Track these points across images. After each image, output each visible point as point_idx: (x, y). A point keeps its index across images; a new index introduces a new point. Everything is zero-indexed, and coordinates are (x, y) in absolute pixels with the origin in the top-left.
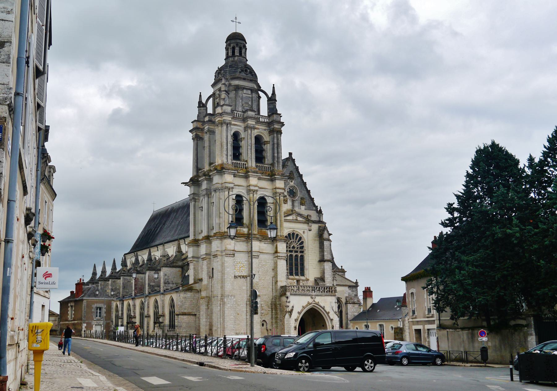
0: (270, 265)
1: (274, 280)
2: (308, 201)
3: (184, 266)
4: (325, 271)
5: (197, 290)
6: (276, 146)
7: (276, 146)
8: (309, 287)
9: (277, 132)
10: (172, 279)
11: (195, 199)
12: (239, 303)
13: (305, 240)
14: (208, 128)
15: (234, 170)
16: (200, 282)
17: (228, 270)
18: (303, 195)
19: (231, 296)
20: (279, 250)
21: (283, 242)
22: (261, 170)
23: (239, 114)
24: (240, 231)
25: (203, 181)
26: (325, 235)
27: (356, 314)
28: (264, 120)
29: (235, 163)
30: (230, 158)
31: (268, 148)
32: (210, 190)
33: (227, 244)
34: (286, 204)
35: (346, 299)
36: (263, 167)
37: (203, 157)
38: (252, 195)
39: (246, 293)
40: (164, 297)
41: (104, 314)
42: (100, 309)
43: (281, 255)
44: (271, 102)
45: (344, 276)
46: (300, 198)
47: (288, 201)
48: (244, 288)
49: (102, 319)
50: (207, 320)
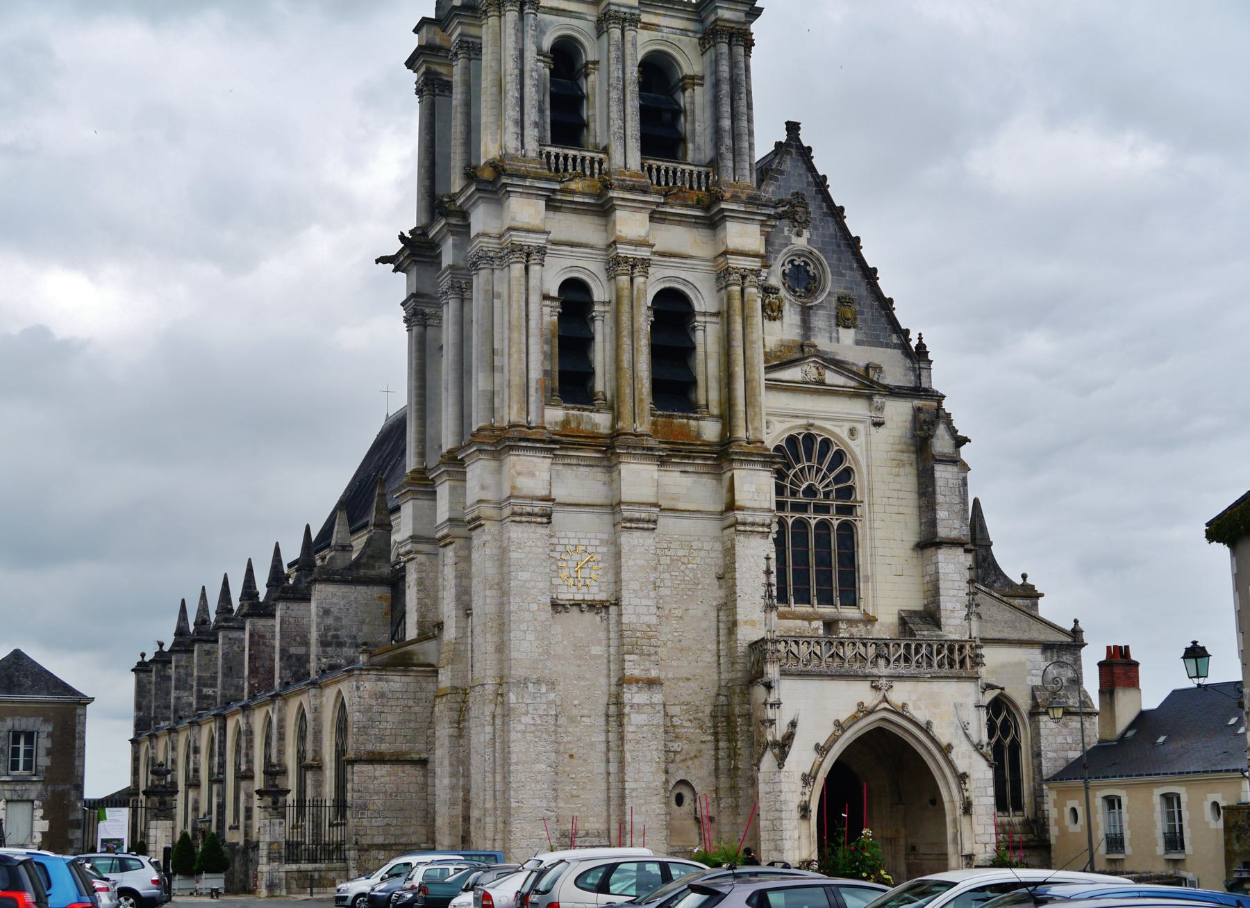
0: (709, 561)
1: (723, 618)
2: (868, 310)
4: (942, 584)
7: (725, 88)
9: (731, 36)
10: (354, 629)
11: (423, 314)
12: (575, 712)
13: (857, 462)
15: (548, 180)
17: (524, 576)
18: (846, 288)
19: (538, 682)
20: (741, 498)
21: (759, 467)
24: (579, 424)
26: (941, 444)
27: (1075, 754)
29: (557, 156)
30: (531, 134)
31: (696, 101)
34: (778, 323)
35: (1034, 698)
39: (605, 672)
40: (321, 696)
41: (43, 761)
42: (30, 737)
43: (750, 519)
45: (1033, 613)
46: (834, 299)
47: (786, 308)
48: (597, 650)
49: (35, 779)
50: (454, 781)
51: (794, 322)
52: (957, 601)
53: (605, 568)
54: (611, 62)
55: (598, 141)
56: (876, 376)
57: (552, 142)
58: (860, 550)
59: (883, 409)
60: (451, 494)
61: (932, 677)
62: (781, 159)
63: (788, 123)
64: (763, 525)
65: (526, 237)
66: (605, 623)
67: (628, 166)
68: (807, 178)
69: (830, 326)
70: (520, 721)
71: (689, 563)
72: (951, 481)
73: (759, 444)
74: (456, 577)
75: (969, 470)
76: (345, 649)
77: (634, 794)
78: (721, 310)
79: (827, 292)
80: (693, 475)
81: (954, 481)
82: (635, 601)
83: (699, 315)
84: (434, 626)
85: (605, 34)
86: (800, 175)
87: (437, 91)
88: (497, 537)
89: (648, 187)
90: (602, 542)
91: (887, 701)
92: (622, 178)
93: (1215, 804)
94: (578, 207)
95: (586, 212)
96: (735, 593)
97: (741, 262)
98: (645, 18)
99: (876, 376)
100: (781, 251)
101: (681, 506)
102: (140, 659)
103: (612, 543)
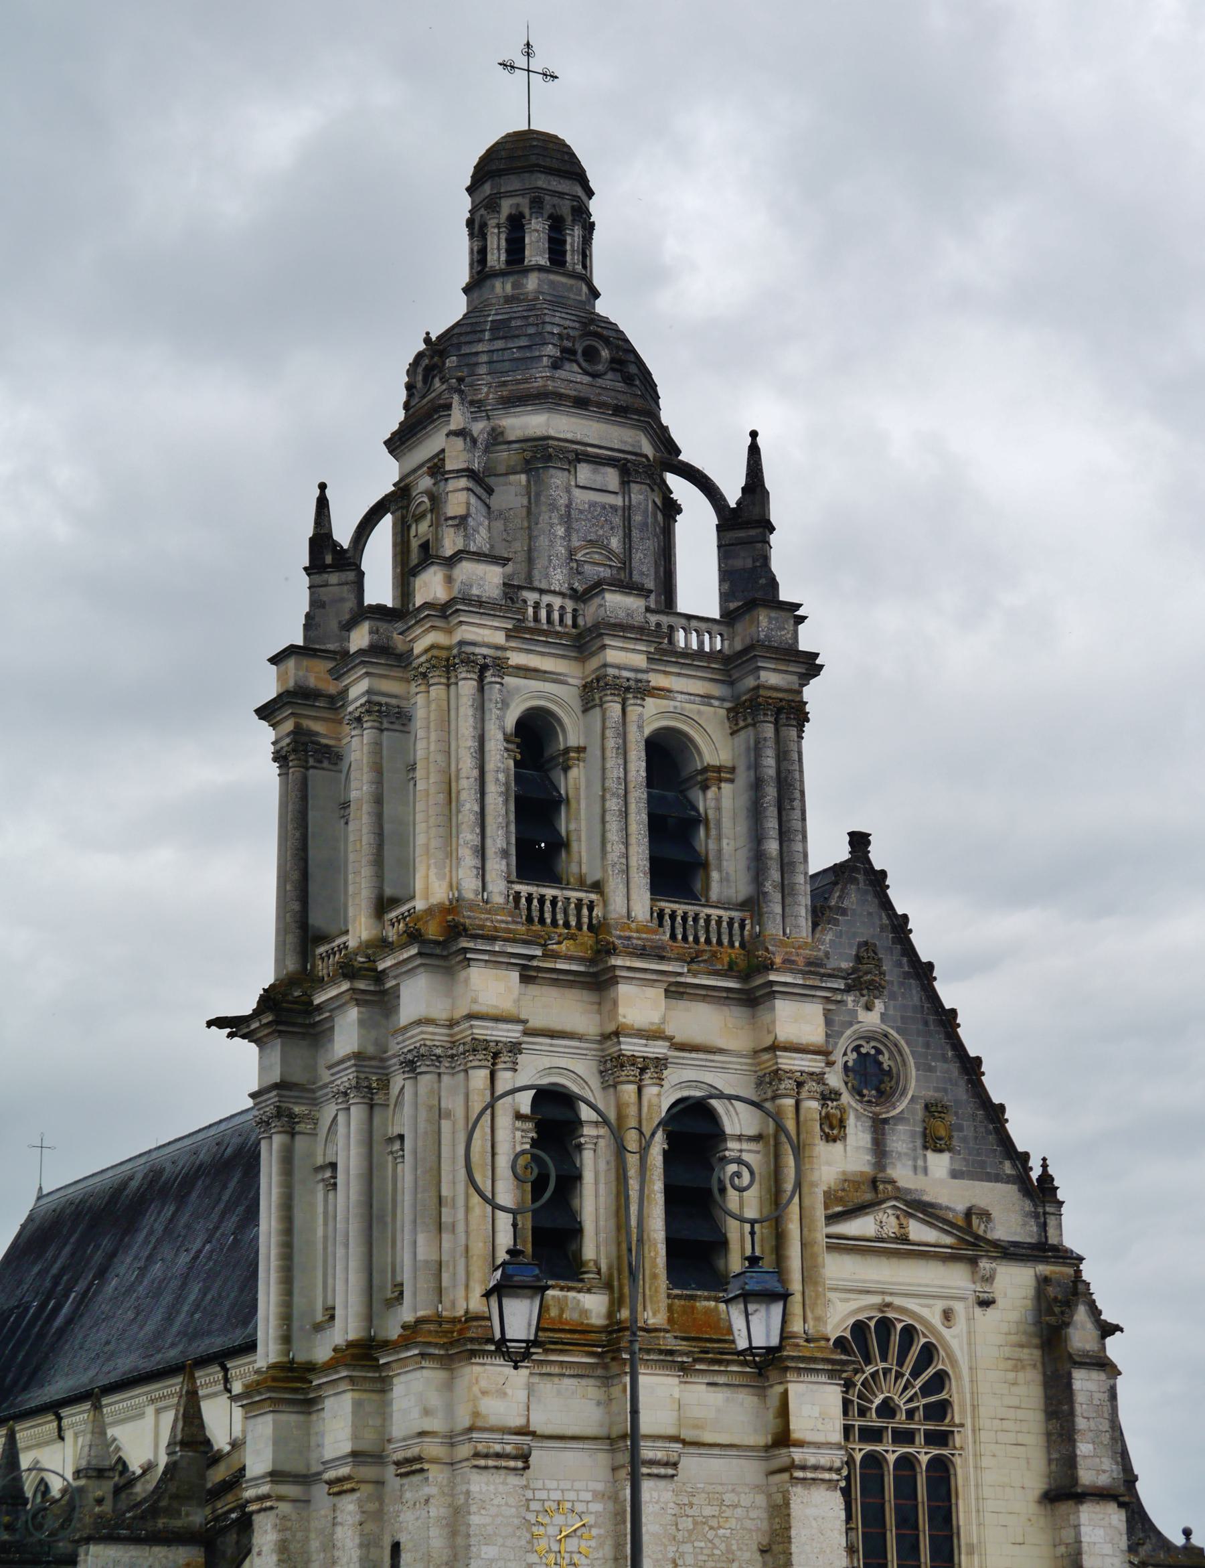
2: (968, 1124)
3: (224, 1531)
7: (771, 792)
9: (779, 711)
11: (291, 1116)
13: (954, 1362)
14: (369, 692)
15: (526, 942)
18: (937, 1089)
20: (799, 1427)
21: (823, 1379)
22: (685, 938)
24: (562, 1311)
25: (336, 1005)
26: (1081, 1336)
28: (701, 643)
29: (529, 899)
30: (497, 867)
32: (383, 1060)
33: (484, 1393)
34: (839, 1146)
37: (336, 867)
38: (632, 1088)
43: (812, 1461)
44: (741, 534)
46: (919, 1107)
47: (851, 1121)
51: (861, 1144)
53: (599, 1536)
54: (608, 754)
55: (584, 870)
56: (982, 1227)
57: (518, 876)
58: (961, 1502)
60: (354, 1413)
62: (842, 891)
63: (852, 835)
64: (830, 1469)
65: (493, 1029)
67: (633, 914)
68: (881, 919)
69: (915, 1150)
71: (720, 1527)
72: (1097, 1396)
73: (823, 1343)
74: (361, 1546)
75: (1120, 1373)
78: (765, 1133)
79: (909, 1096)
80: (725, 1389)
81: (1101, 1396)
83: (733, 1140)
85: (598, 709)
86: (870, 914)
87: (311, 762)
88: (446, 1490)
89: (663, 948)
90: (598, 1496)
92: (627, 934)
94: (561, 977)
95: (571, 984)
97: (796, 1062)
99: (982, 1227)
100: (842, 1033)
101: (708, 1438)
103: (609, 1498)
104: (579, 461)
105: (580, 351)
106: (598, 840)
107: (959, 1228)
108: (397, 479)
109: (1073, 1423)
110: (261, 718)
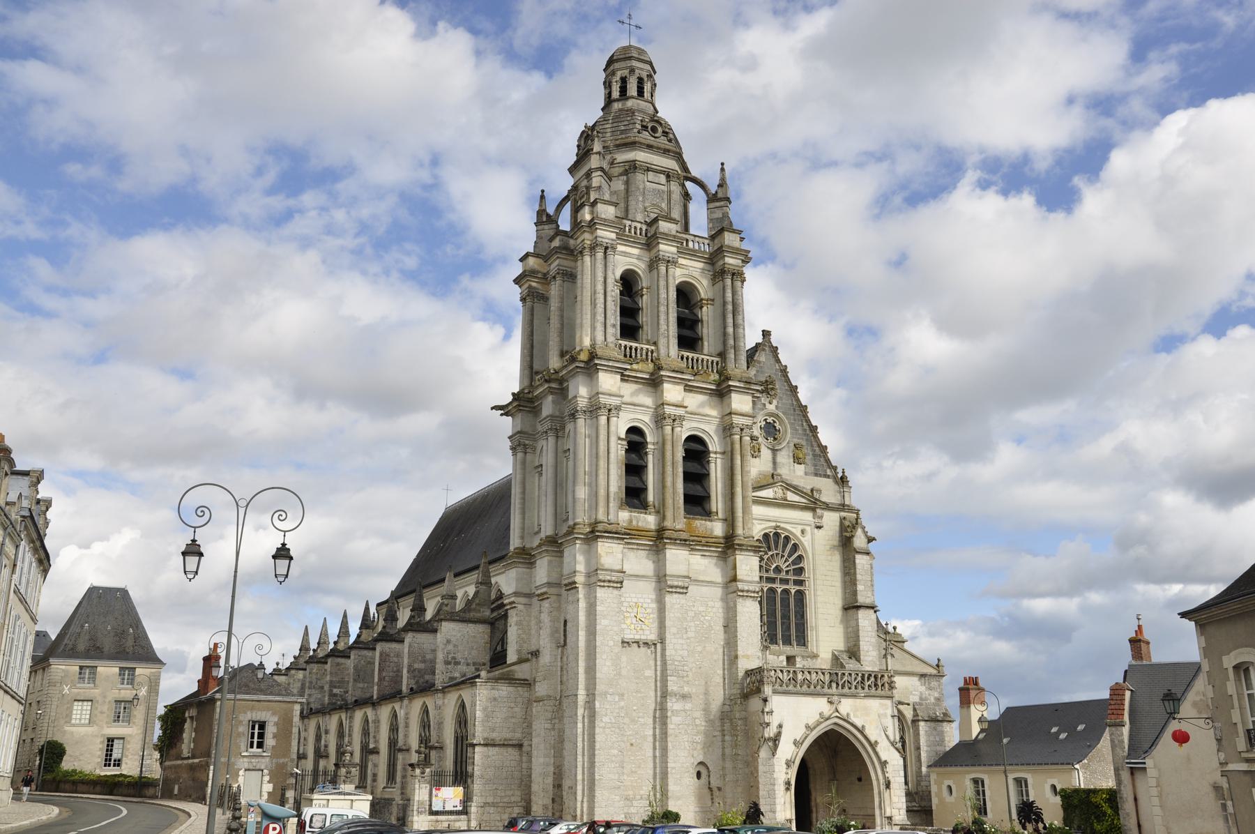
4: (861, 634)
5: (527, 680)
6: (730, 307)
7: (730, 307)
8: (823, 673)
9: (733, 274)
11: (525, 445)
14: (558, 265)
16: (534, 659)
20: (741, 573)
21: (752, 554)
22: (693, 368)
23: (635, 228)
24: (638, 522)
26: (859, 541)
28: (700, 247)
32: (562, 418)
36: (697, 361)
37: (545, 344)
38: (670, 428)
39: (653, 688)
40: (444, 699)
41: (269, 741)
42: (262, 726)
43: (746, 588)
44: (718, 204)
46: (792, 445)
48: (649, 673)
49: (265, 754)
52: (870, 645)
55: (649, 338)
59: (822, 517)
61: (865, 696)
66: (654, 654)
70: (601, 720)
71: (706, 616)
76: (459, 667)
77: (674, 771)
82: (673, 641)
84: (528, 653)
91: (838, 711)
93: (1054, 787)
96: (737, 637)
98: (681, 261)
101: (701, 578)
102: (275, 666)
104: (649, 171)
105: (649, 127)
106: (656, 324)
107: (808, 495)
108: (572, 184)
109: (856, 577)
110: (516, 284)
